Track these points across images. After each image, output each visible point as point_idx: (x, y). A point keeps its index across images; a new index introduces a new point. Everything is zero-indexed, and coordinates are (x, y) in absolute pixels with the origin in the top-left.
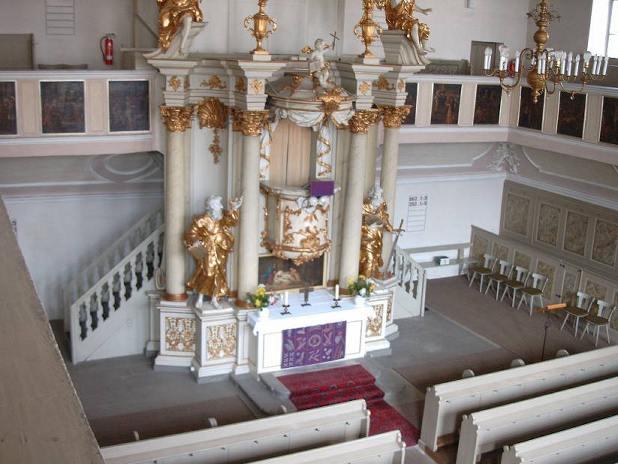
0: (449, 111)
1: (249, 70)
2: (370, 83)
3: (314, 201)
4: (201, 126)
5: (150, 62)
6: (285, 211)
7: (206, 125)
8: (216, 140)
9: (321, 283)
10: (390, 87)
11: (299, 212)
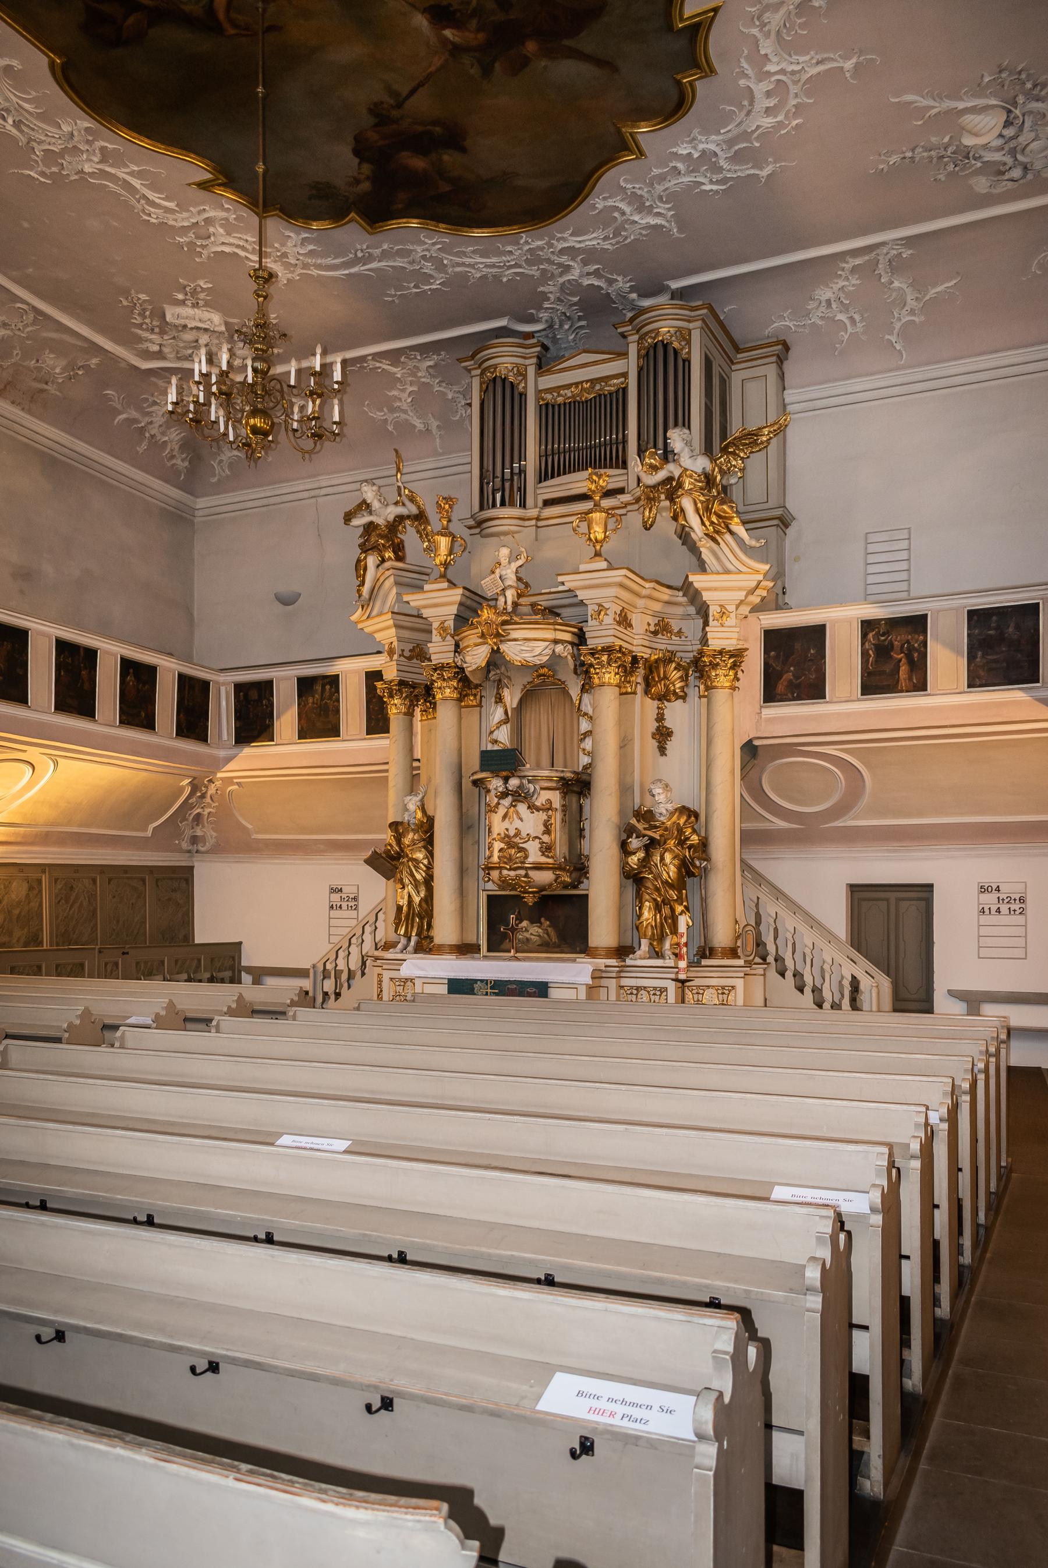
1: (425, 607)
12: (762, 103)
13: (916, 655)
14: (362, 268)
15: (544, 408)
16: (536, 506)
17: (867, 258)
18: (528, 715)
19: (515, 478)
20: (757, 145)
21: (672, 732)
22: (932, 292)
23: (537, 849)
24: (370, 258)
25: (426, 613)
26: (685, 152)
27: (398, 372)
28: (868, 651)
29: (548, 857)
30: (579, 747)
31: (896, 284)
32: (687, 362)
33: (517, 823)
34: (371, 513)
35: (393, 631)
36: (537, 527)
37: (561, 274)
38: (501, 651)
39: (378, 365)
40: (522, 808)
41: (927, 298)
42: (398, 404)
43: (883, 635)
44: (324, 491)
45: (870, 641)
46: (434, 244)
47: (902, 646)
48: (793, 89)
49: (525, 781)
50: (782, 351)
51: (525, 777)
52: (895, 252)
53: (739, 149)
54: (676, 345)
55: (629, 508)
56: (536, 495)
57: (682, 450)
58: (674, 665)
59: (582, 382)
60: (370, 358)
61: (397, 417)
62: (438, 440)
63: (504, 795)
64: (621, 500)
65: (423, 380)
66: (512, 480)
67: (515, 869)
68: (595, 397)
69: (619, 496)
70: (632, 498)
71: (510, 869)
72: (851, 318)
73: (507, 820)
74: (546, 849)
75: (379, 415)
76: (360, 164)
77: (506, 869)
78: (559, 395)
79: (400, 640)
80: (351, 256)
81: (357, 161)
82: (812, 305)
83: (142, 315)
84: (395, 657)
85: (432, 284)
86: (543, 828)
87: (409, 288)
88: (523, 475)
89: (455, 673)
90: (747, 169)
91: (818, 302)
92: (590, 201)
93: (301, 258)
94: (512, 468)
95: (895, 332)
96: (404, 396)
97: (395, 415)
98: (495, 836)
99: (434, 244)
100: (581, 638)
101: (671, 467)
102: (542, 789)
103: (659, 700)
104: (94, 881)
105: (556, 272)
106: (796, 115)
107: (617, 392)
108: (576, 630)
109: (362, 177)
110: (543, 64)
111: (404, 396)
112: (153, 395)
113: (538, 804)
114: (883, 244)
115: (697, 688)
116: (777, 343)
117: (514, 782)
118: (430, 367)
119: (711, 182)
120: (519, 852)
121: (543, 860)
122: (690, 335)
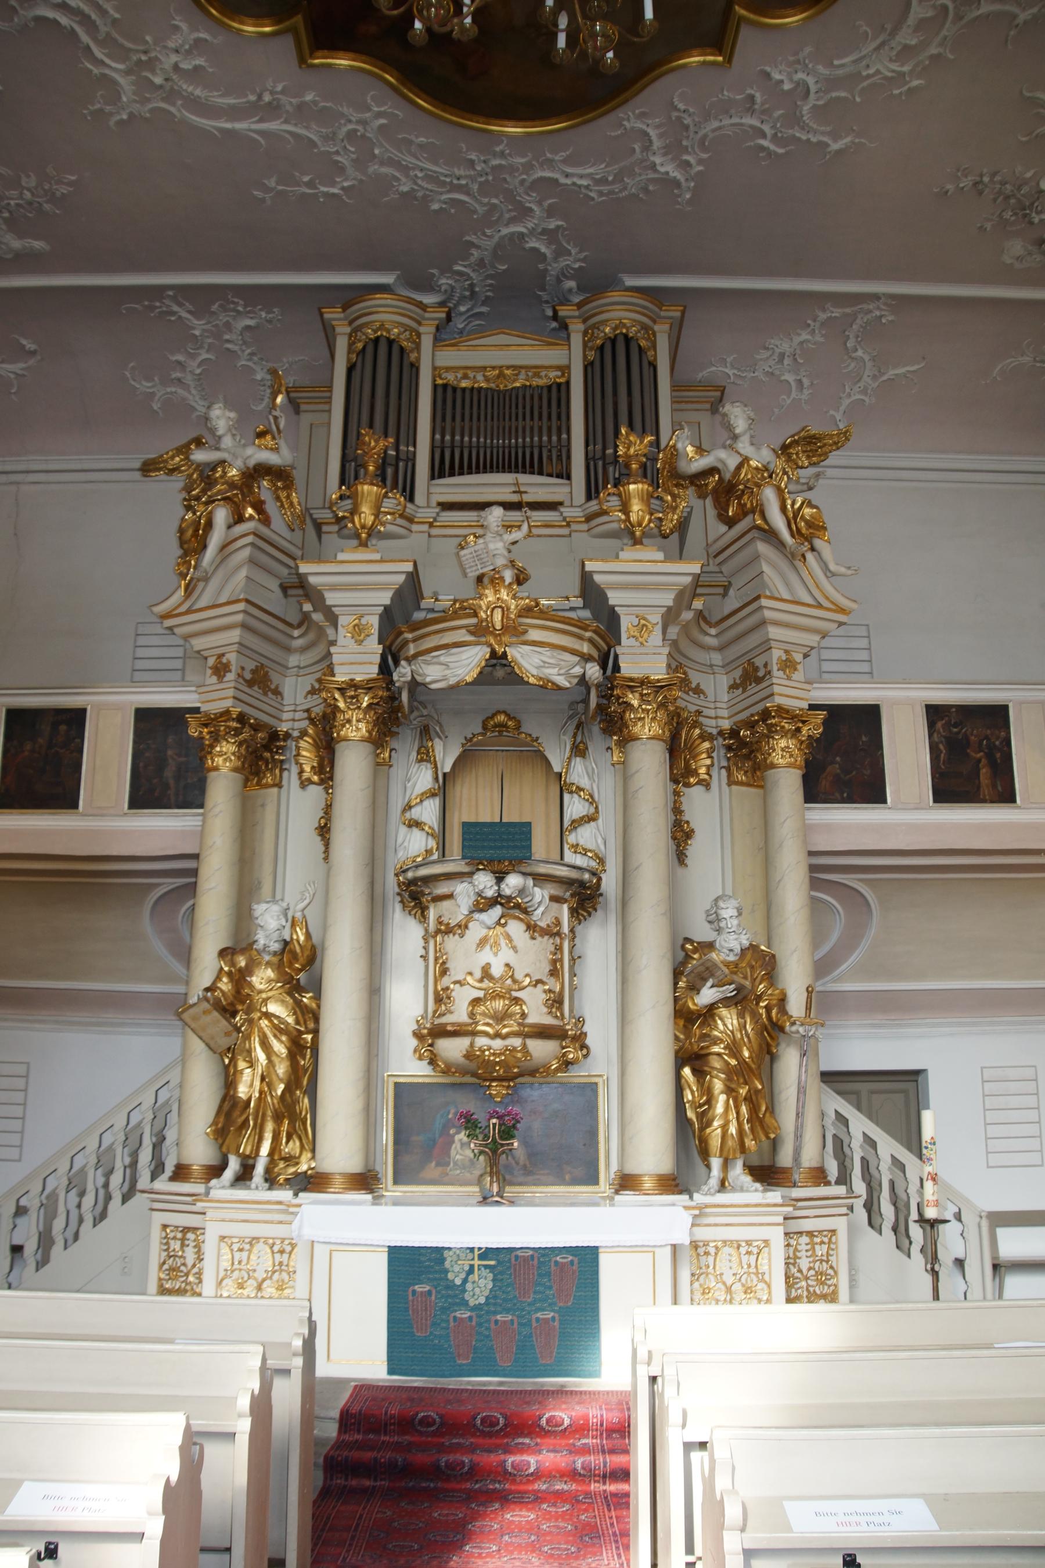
0: (984, 772)
1: (334, 588)
2: (656, 618)
3: (484, 881)
4: (304, 784)
6: (438, 931)
7: (310, 782)
8: (328, 809)
10: (761, 674)
11: (463, 926)
13: (998, 755)
14: (254, 127)
15: (440, 391)
16: (428, 507)
17: (848, 310)
18: (458, 788)
19: (401, 464)
21: (692, 831)
22: (892, 373)
23: (540, 1002)
25: (332, 598)
27: (199, 327)
28: (937, 744)
29: (556, 1017)
31: (860, 353)
32: (653, 366)
33: (506, 955)
34: (218, 449)
37: (512, 221)
39: (175, 308)
40: (516, 928)
41: (885, 378)
42: (178, 375)
43: (955, 725)
44: (32, 477)
45: (939, 733)
46: (379, 115)
47: (980, 742)
49: (530, 882)
51: (530, 874)
52: (878, 313)
53: (838, 98)
55: (574, 527)
56: (429, 493)
57: (745, 433)
58: (697, 731)
59: (501, 367)
60: (171, 293)
61: (171, 393)
63: (483, 904)
64: (565, 514)
69: (562, 509)
70: (581, 514)
71: (497, 1035)
72: (800, 382)
73: (488, 947)
74: (556, 1002)
75: (145, 386)
77: (486, 1034)
78: (465, 377)
80: (252, 98)
82: (765, 354)
84: (230, 676)
85: (333, 184)
86: (547, 967)
88: (410, 464)
89: (381, 698)
90: (823, 133)
91: (770, 352)
92: (620, 113)
95: (842, 408)
96: (193, 364)
97: (169, 390)
98: (460, 977)
99: (379, 115)
100: (607, 660)
102: (554, 899)
105: (507, 216)
107: (549, 387)
111: (193, 364)
113: (543, 924)
114: (876, 297)
115: (724, 772)
117: (513, 882)
118: (248, 328)
119: (775, 138)
120: (516, 1004)
121: (548, 1020)
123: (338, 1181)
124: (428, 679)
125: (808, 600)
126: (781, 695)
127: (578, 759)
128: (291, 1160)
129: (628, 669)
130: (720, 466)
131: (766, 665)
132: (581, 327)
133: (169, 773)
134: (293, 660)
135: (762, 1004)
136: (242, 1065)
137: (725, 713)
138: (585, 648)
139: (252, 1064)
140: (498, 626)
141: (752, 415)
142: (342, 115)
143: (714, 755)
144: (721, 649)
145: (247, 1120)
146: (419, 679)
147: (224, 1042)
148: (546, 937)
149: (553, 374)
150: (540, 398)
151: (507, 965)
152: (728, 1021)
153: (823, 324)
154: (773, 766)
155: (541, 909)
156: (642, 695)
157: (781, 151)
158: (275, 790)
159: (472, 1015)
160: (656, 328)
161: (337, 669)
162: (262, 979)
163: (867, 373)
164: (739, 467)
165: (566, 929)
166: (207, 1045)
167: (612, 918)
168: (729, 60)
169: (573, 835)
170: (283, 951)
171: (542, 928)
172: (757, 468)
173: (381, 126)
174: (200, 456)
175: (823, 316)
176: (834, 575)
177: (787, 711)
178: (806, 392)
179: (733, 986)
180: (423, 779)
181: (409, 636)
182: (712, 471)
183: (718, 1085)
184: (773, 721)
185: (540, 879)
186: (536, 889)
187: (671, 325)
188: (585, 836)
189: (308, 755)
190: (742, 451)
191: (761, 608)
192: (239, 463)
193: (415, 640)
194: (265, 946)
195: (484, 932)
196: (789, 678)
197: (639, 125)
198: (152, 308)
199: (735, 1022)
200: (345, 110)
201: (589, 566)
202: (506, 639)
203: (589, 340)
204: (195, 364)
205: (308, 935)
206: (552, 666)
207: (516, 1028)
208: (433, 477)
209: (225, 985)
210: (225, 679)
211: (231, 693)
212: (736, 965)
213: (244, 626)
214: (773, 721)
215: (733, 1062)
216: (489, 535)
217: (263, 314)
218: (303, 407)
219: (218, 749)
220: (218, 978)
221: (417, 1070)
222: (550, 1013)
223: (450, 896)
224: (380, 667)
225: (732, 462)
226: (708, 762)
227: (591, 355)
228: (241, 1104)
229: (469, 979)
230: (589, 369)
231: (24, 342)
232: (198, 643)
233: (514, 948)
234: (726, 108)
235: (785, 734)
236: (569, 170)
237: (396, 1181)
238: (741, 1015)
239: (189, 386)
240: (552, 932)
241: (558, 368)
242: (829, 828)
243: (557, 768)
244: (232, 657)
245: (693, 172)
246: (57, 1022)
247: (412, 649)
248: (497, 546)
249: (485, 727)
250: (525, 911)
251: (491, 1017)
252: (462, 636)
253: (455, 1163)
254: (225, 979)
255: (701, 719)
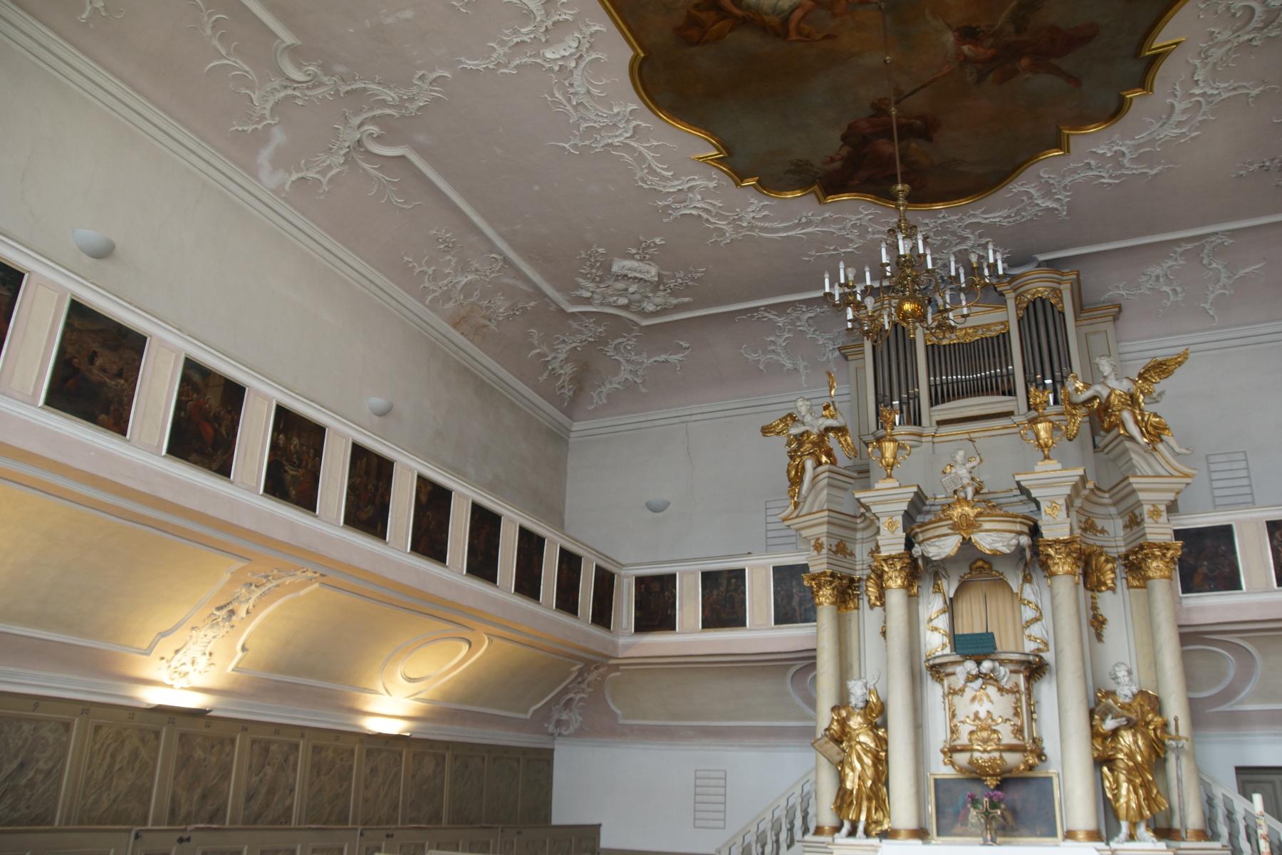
1: (875, 503)
3: (970, 666)
4: (872, 606)
5: (805, 533)
6: (950, 693)
7: (875, 605)
9: (1054, 834)
10: (1139, 520)
11: (962, 691)
12: (1177, 117)
15: (930, 348)
16: (931, 426)
17: (1197, 244)
19: (911, 401)
20: (1159, 150)
21: (1106, 620)
22: (1242, 272)
24: (809, 223)
25: (874, 509)
26: (1102, 152)
27: (781, 321)
30: (1023, 633)
31: (1214, 265)
32: (1062, 313)
34: (803, 423)
35: (824, 528)
36: (933, 443)
38: (973, 541)
40: (992, 690)
41: (1237, 276)
42: (773, 348)
44: (694, 418)
45: (1277, 539)
46: (867, 215)
48: (1204, 108)
49: (997, 664)
50: (1116, 312)
51: (997, 660)
52: (1220, 241)
53: (1144, 152)
54: (1053, 301)
56: (930, 416)
57: (1110, 374)
58: (1103, 558)
62: (804, 378)
63: (971, 678)
65: (801, 328)
66: (909, 404)
67: (989, 752)
68: (977, 340)
69: (1013, 417)
71: (985, 751)
72: (1174, 290)
73: (976, 702)
74: (1019, 731)
76: (842, 146)
79: (829, 535)
80: (796, 221)
81: (841, 143)
82: (1144, 278)
83: (592, 267)
84: (824, 551)
85: (848, 247)
86: (1011, 711)
87: (828, 250)
88: (917, 400)
93: (753, 221)
94: (908, 393)
95: (1209, 301)
96: (780, 341)
97: (768, 357)
98: (962, 719)
99: (867, 215)
100: (1035, 531)
101: (1098, 388)
102: (1012, 672)
103: (1092, 590)
104: (483, 759)
105: (954, 242)
106: (1197, 129)
107: (998, 337)
108: (1032, 523)
109: (839, 157)
110: (1027, 76)
111: (780, 341)
112: (564, 335)
113: (1007, 687)
114: (1216, 233)
115: (1124, 581)
116: (1115, 306)
117: (986, 665)
119: (1110, 177)
121: (1015, 742)
122: (1061, 294)
123: (903, 833)
124: (930, 555)
125: (1163, 472)
126: (1151, 533)
127: (1027, 585)
128: (878, 823)
129: (1048, 534)
130: (1096, 394)
131: (1141, 515)
132: (1013, 295)
133: (795, 602)
134: (859, 535)
135: (1151, 727)
136: (847, 770)
137: (1122, 543)
138: (1018, 527)
139: (853, 770)
140: (965, 525)
141: (1113, 363)
142: (847, 219)
143: (1117, 571)
144: (1115, 504)
145: (852, 801)
146: (925, 554)
147: (838, 758)
148: (1010, 695)
149: (998, 328)
150: (993, 343)
151: (988, 712)
152: (1127, 738)
153: (1181, 255)
154: (1149, 578)
155: (1006, 679)
156: (1056, 549)
157: (1116, 182)
158: (856, 611)
159: (970, 740)
160: (1062, 287)
161: (882, 549)
162: (856, 722)
163: (1223, 275)
164: (1109, 396)
165: (1022, 687)
166: (829, 760)
167: (1054, 677)
168: (1068, 152)
169: (1028, 630)
170: (866, 707)
171: (1007, 689)
172: (1120, 395)
173: (870, 219)
174: (795, 431)
175: (1179, 250)
176: (1179, 454)
177: (1155, 544)
178: (1180, 295)
179: (1124, 719)
180: (937, 603)
181: (918, 530)
182: (1094, 398)
183: (1122, 777)
184: (1145, 551)
185: (1002, 662)
186: (1002, 668)
187: (1071, 284)
188: (1036, 630)
189: (872, 590)
190: (1110, 385)
191: (1130, 484)
192: (815, 431)
193: (922, 532)
194: (856, 705)
195: (973, 693)
196: (1156, 522)
197: (1022, 189)
198: (753, 317)
199: (1131, 739)
200: (848, 217)
201: (1018, 478)
202: (969, 531)
203: (1019, 303)
204: (782, 341)
205: (878, 698)
206: (998, 542)
207: (995, 747)
208: (932, 405)
209: (835, 726)
210: (822, 553)
211: (825, 560)
212: (1130, 705)
213: (829, 523)
214: (1145, 551)
215: (1131, 764)
216: (958, 467)
217: (818, 310)
218: (850, 358)
219: (821, 593)
220: (832, 723)
221: (946, 772)
222: (1016, 737)
223: (953, 674)
224: (906, 545)
225: (1105, 393)
226: (1112, 576)
227: (1021, 313)
228: (849, 792)
229: (968, 720)
230: (1021, 322)
231: (682, 343)
232: (805, 533)
233: (991, 702)
234: (1074, 171)
235: (1155, 557)
236: (986, 216)
237: (938, 835)
238: (1134, 735)
239: (779, 353)
240: (1014, 691)
241: (1002, 323)
242: (1202, 609)
243: (1015, 590)
244: (824, 540)
245: (1064, 202)
246: (740, 746)
247: (920, 537)
248: (963, 472)
249: (971, 569)
250: (996, 680)
251: (981, 741)
252: (946, 530)
253: (972, 824)
254: (835, 723)
255: (1105, 549)
